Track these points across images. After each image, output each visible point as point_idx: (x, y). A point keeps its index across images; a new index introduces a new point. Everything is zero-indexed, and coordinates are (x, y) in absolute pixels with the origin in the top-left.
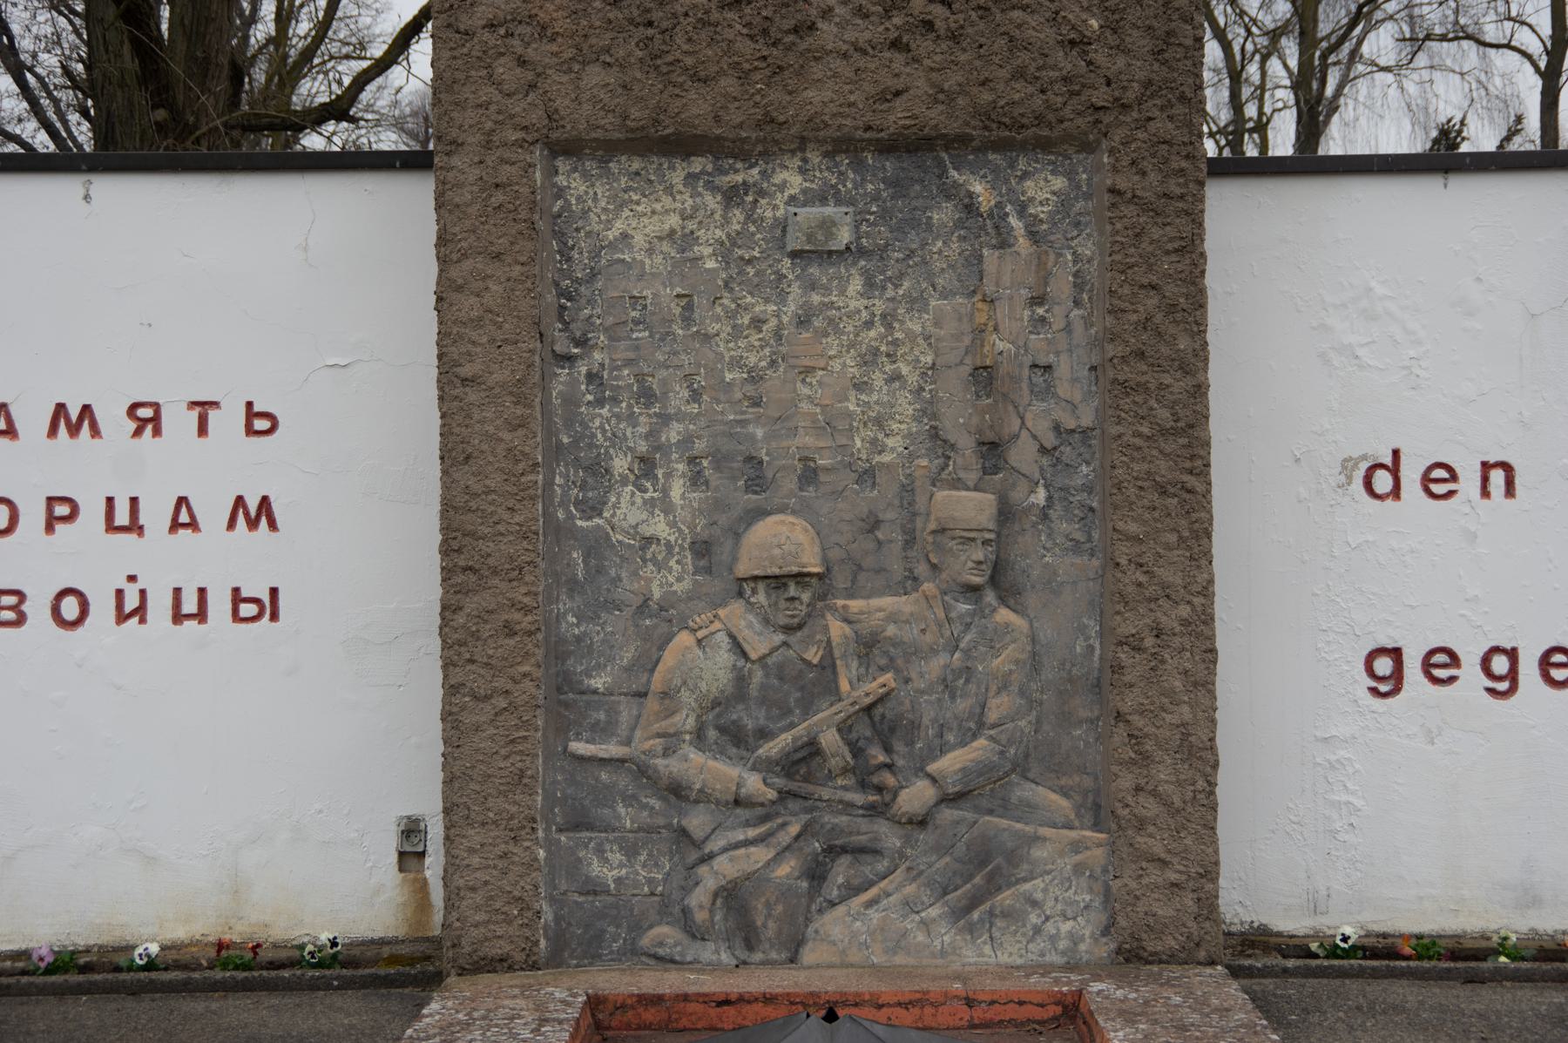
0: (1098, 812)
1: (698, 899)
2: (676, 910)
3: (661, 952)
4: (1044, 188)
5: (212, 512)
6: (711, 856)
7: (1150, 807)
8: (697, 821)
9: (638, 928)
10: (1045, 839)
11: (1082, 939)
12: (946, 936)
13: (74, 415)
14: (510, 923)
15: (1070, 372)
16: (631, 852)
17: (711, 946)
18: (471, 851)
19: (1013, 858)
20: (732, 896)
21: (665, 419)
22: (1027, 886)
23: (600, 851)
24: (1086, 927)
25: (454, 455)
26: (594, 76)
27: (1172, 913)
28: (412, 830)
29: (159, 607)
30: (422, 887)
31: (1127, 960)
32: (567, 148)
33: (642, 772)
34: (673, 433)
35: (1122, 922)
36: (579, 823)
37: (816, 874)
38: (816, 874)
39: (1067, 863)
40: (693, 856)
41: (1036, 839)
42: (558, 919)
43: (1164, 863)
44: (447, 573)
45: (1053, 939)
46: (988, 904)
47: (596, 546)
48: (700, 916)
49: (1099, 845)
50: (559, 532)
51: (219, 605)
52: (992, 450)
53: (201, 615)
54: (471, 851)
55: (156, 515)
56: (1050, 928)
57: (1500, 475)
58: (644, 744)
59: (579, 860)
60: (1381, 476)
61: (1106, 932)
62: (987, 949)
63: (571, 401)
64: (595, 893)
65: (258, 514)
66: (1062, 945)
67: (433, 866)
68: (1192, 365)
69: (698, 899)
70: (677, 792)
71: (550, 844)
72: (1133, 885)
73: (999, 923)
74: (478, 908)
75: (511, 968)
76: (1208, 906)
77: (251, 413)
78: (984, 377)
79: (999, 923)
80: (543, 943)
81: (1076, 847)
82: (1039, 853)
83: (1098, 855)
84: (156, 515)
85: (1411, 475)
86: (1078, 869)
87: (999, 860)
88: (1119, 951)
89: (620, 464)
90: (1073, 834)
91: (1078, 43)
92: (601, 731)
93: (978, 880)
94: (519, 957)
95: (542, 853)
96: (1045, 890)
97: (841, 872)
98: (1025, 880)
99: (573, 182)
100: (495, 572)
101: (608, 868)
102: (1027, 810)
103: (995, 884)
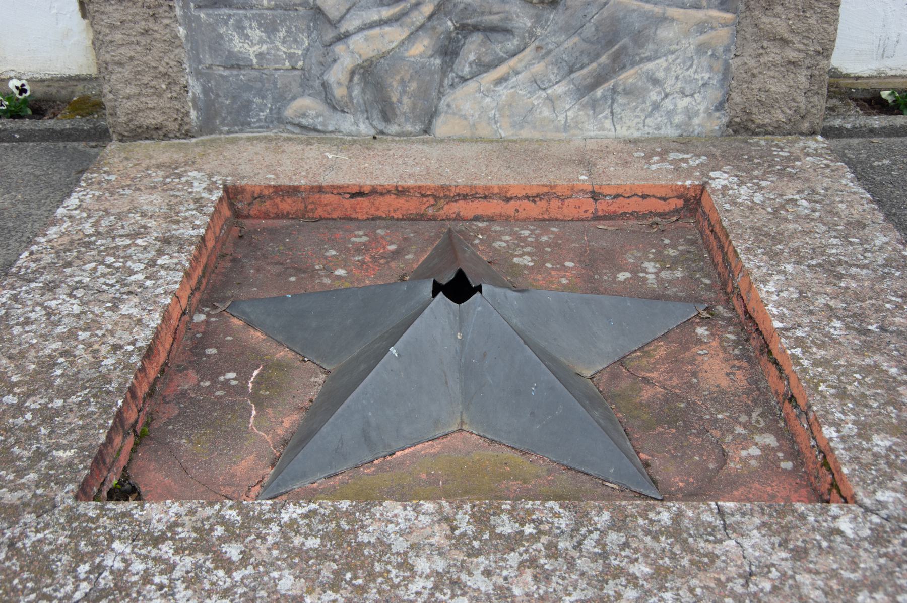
1: (337, 75)
2: (317, 83)
3: (304, 122)
6: (347, 35)
9: (282, 99)
10: (672, 20)
11: (697, 114)
12: (570, 111)
14: (160, 96)
16: (270, 28)
17: (350, 118)
18: (112, 27)
19: (639, 38)
20: (368, 73)
22: (650, 66)
23: (239, 28)
24: (702, 103)
27: (783, 88)
31: (736, 132)
35: (737, 98)
37: (449, 51)
38: (449, 51)
39: (691, 44)
40: (330, 35)
41: (664, 19)
42: (206, 91)
43: (785, 42)
45: (670, 114)
48: (339, 92)
49: (725, 25)
54: (112, 27)
56: (668, 104)
59: (221, 36)
61: (720, 107)
62: (608, 124)
64: (239, 67)
66: (678, 119)
69: (337, 75)
71: (189, 21)
72: (752, 63)
73: (621, 100)
74: (128, 82)
75: (166, 136)
79: (621, 100)
80: (193, 114)
81: (702, 27)
82: (665, 33)
83: (723, 35)
86: (701, 49)
87: (626, 41)
88: (729, 125)
90: (700, 14)
93: (604, 59)
94: (173, 126)
95: (182, 31)
96: (667, 69)
97: (473, 49)
98: (649, 59)
101: (249, 44)
103: (619, 63)
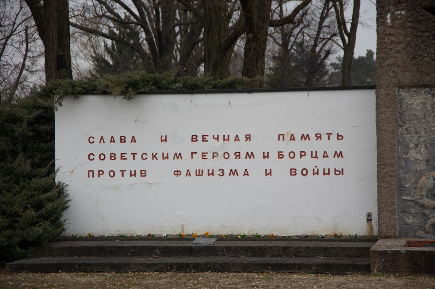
1: (427, 226)
2: (423, 228)
3: (420, 236)
5: (331, 154)
6: (430, 218)
8: (427, 212)
9: (415, 231)
13: (305, 136)
14: (391, 230)
16: (414, 217)
17: (430, 235)
18: (384, 216)
21: (420, 137)
23: (408, 217)
25: (379, 144)
26: (407, 74)
28: (369, 215)
29: (321, 172)
30: (371, 226)
32: (402, 87)
33: (416, 202)
34: (422, 140)
36: (404, 212)
40: (426, 218)
42: (400, 229)
44: (378, 166)
47: (407, 161)
48: (428, 229)
50: (400, 158)
51: (332, 172)
53: (329, 174)
54: (384, 216)
55: (320, 155)
58: (416, 197)
59: (404, 219)
63: (402, 134)
64: (407, 225)
65: (340, 155)
67: (374, 222)
69: (427, 226)
70: (423, 206)
71: (398, 215)
74: (385, 227)
75: (391, 238)
77: (338, 136)
80: (397, 233)
84: (320, 155)
89: (412, 145)
92: (408, 195)
94: (393, 236)
95: (397, 217)
99: (403, 93)
100: (388, 165)
101: (410, 220)
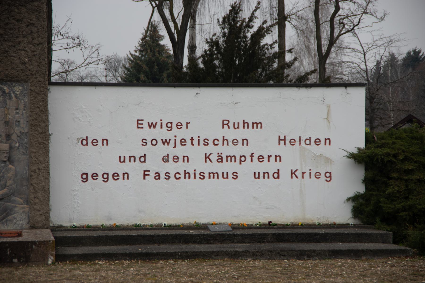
0: (27, 202)
4: (18, 89)
7: (37, 201)
10: (17, 207)
11: (24, 224)
15: (23, 123)
22: (14, 215)
31: (32, 228)
35: (31, 221)
39: (21, 211)
41: (15, 207)
43: (39, 211)
45: (18, 225)
46: (6, 219)
49: (27, 207)
52: (8, 136)
56: (18, 223)
57: (105, 141)
60: (84, 141)
61: (28, 223)
62: (6, 227)
66: (20, 226)
68: (46, 122)
72: (33, 214)
73: (8, 222)
76: (48, 218)
78: (7, 123)
79: (8, 222)
81: (23, 208)
82: (16, 209)
83: (27, 209)
85: (90, 141)
86: (23, 212)
87: (8, 211)
88: (30, 226)
90: (23, 206)
91: (24, 63)
93: (4, 214)
96: (17, 216)
98: (13, 214)
102: (14, 202)
103: (8, 215)
